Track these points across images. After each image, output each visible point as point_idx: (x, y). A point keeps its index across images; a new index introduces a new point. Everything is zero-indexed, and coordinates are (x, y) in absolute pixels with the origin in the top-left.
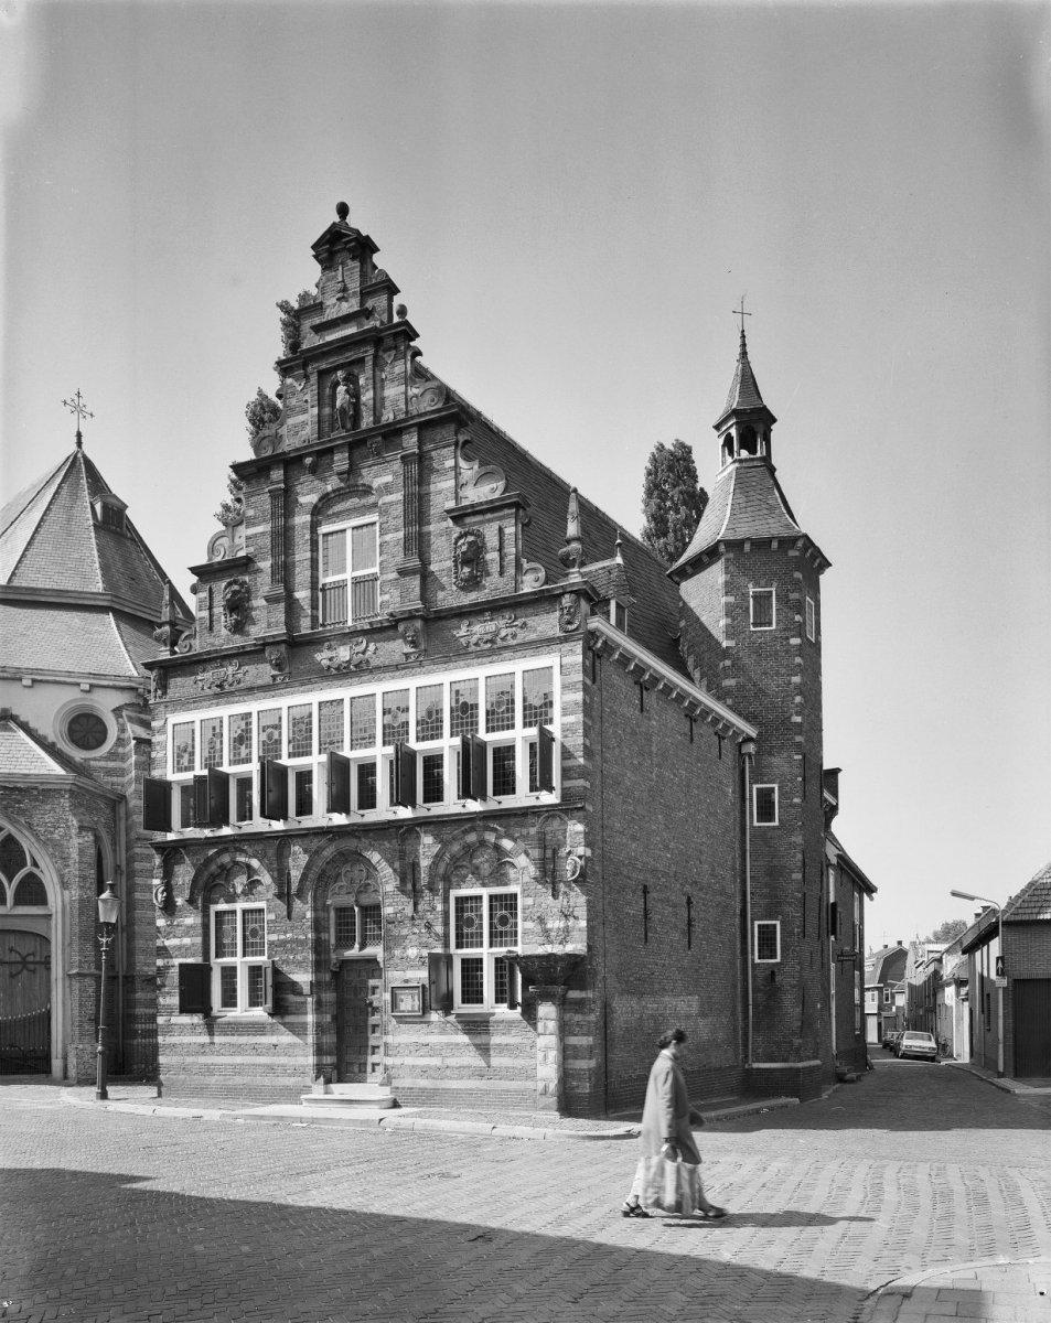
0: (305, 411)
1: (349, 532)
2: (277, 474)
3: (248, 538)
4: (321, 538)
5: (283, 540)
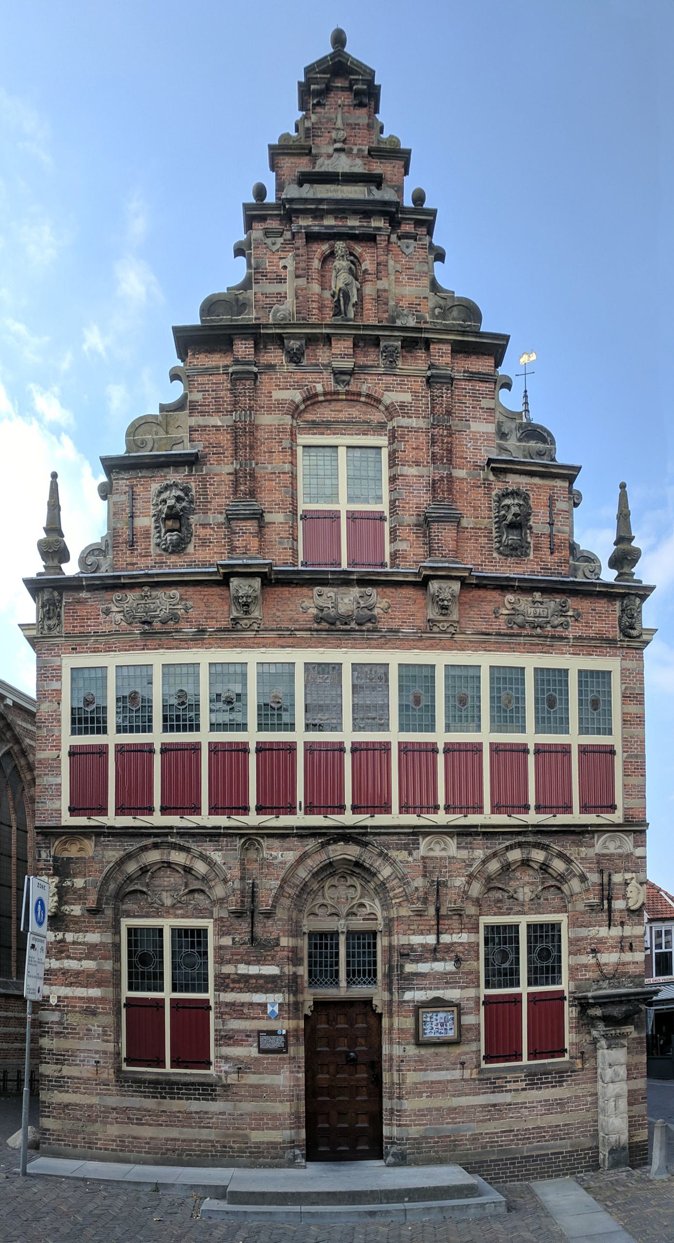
0: (281, 280)
1: (342, 451)
2: (243, 348)
3: (192, 430)
4: (300, 450)
5: (244, 438)
